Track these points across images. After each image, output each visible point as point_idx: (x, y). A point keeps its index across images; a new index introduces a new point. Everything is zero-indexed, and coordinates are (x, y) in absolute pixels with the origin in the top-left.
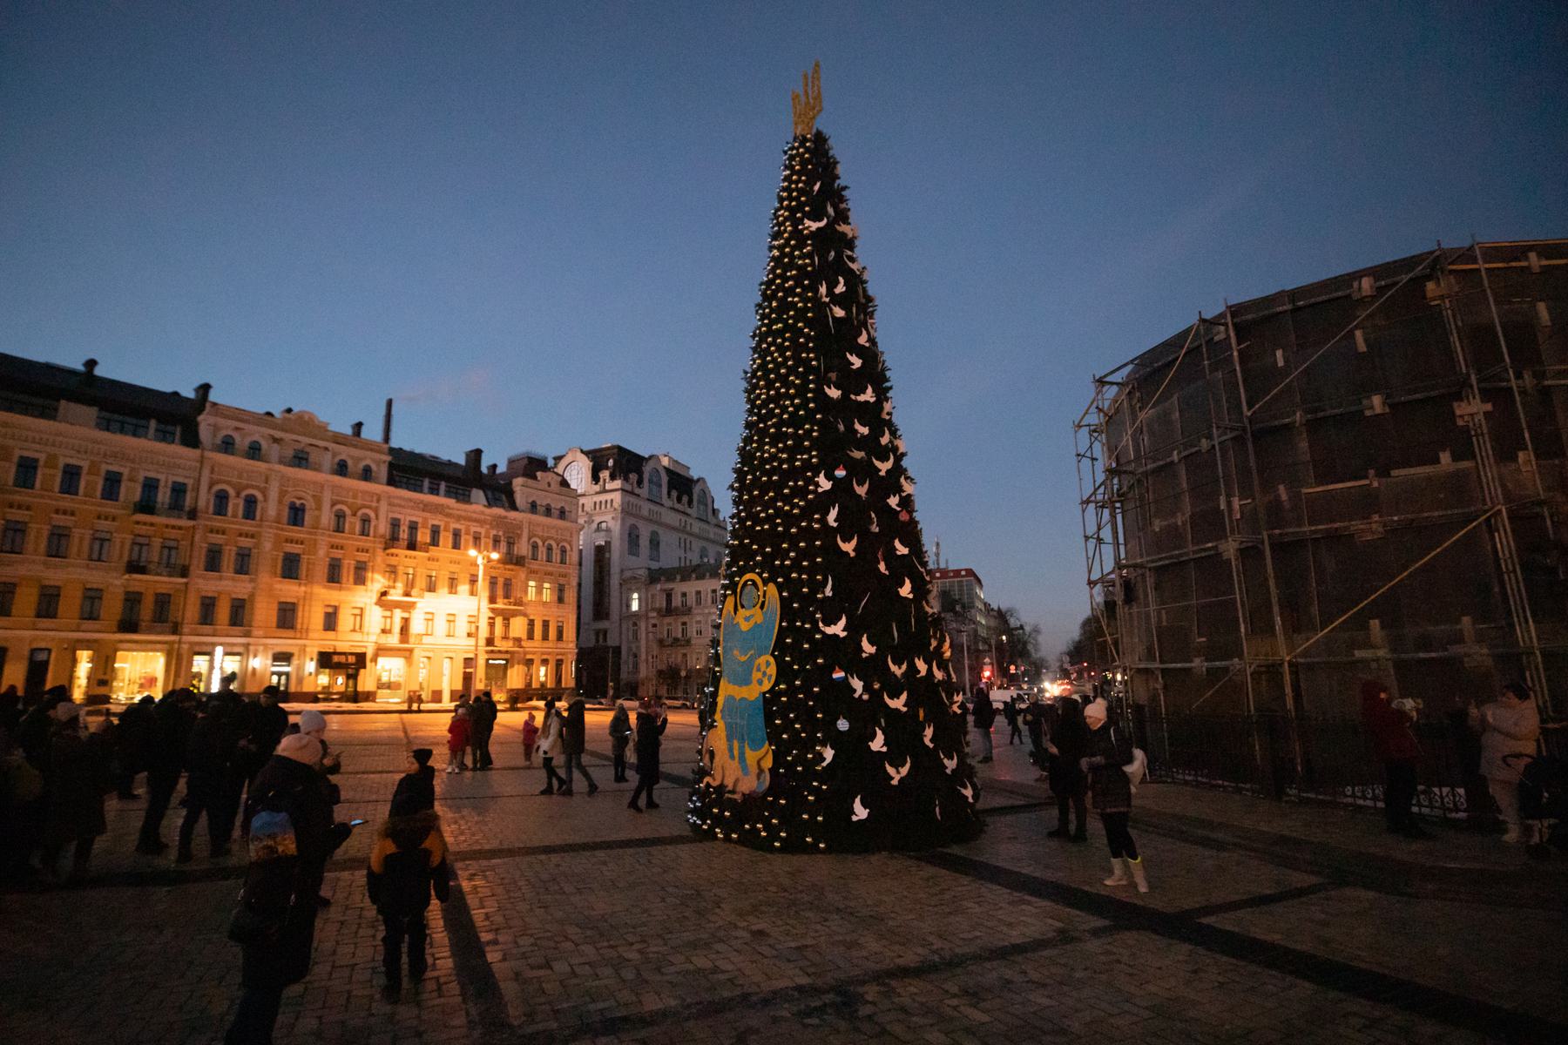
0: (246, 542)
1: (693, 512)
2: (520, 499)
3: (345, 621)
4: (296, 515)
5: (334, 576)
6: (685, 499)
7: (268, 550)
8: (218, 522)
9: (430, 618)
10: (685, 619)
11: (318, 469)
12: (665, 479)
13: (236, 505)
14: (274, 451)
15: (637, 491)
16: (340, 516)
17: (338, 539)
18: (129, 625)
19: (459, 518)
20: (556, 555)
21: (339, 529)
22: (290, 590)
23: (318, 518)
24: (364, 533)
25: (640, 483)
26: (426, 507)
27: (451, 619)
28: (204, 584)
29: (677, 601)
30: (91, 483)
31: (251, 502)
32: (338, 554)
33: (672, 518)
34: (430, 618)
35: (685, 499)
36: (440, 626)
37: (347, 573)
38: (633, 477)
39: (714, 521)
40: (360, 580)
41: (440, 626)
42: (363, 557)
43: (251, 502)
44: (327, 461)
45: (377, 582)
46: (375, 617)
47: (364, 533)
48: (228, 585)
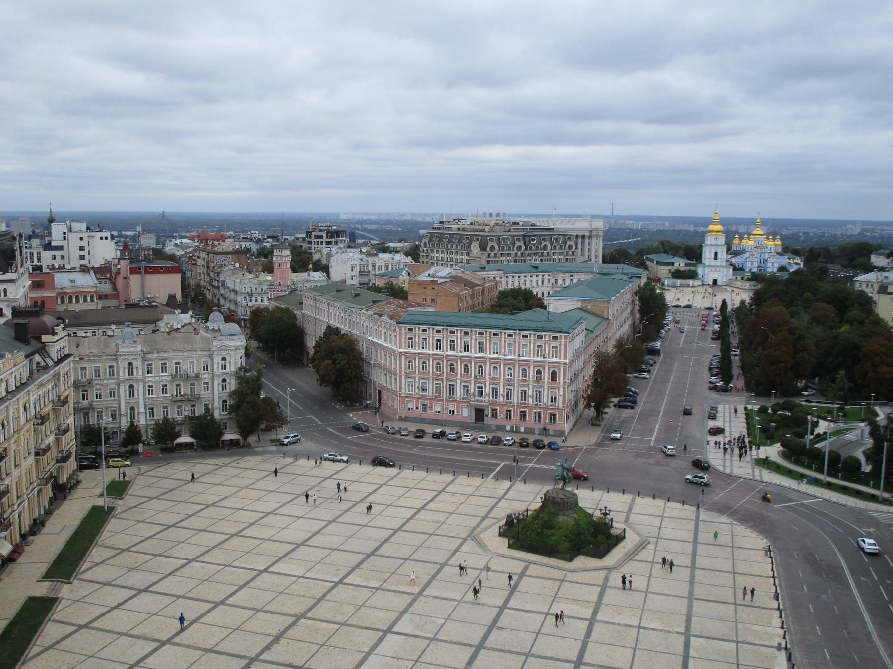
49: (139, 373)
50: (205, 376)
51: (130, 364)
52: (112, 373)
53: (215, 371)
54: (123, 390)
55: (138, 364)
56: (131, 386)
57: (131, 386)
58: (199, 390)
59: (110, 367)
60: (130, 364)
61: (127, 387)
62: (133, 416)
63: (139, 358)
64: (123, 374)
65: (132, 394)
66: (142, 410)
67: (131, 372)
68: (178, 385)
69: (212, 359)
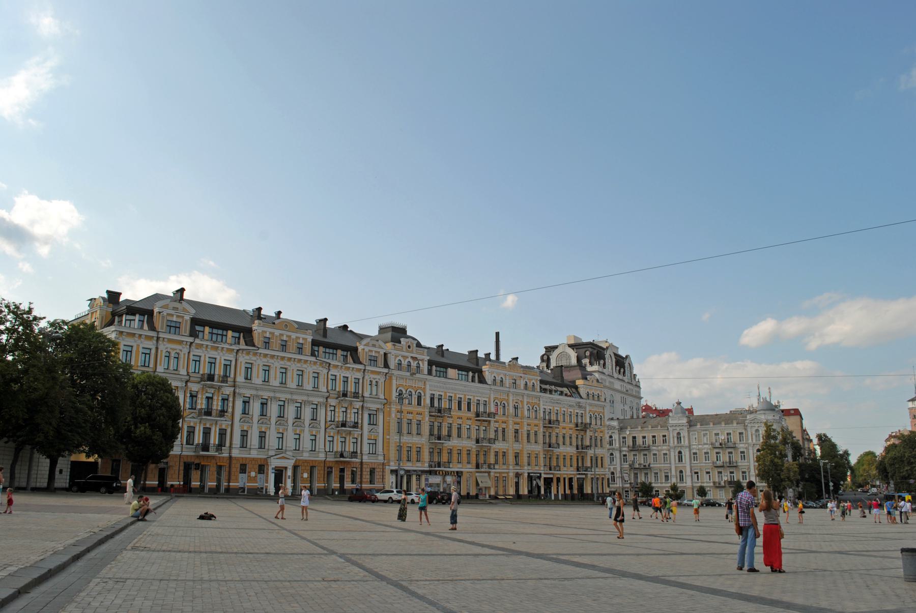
0: (504, 426)
1: (625, 378)
2: (583, 391)
6: (622, 370)
10: (645, 452)
12: (614, 360)
14: (508, 382)
15: (605, 371)
20: (599, 423)
23: (523, 413)
25: (604, 365)
29: (639, 441)
30: (464, 406)
33: (618, 385)
35: (622, 370)
38: (602, 362)
39: (634, 383)
49: (684, 442)
50: (742, 446)
51: (679, 434)
52: (664, 441)
53: (750, 441)
54: (673, 455)
55: (684, 434)
56: (680, 452)
57: (680, 452)
58: (736, 457)
59: (664, 436)
60: (679, 434)
61: (677, 453)
62: (682, 479)
63: (686, 429)
64: (673, 442)
65: (680, 459)
66: (688, 473)
67: (679, 439)
68: (717, 453)
69: (746, 429)
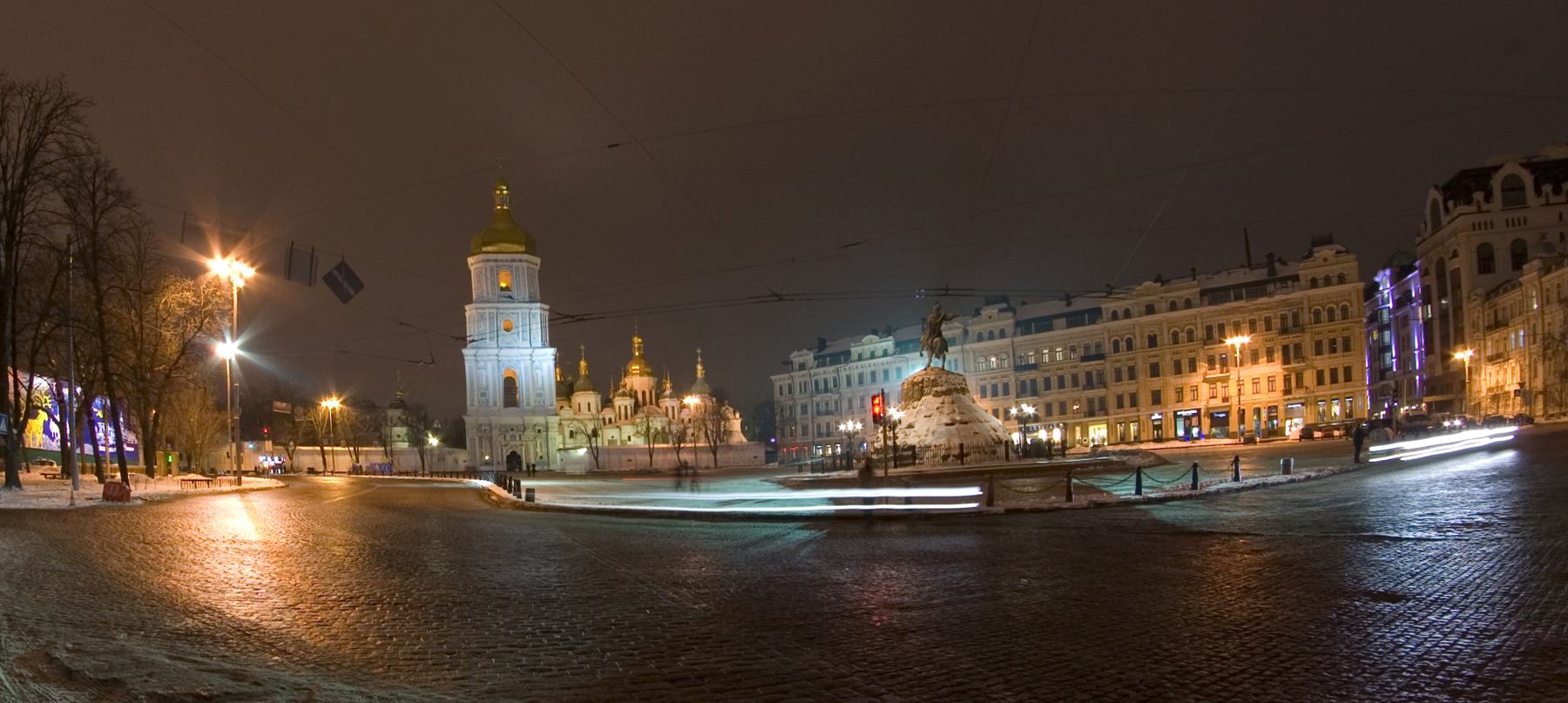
0: (1131, 363)
3: (1188, 396)
4: (1153, 341)
5: (1178, 370)
7: (1142, 367)
8: (1116, 357)
9: (1240, 383)
11: (1160, 311)
13: (1123, 345)
16: (1175, 335)
17: (1177, 348)
18: (1091, 414)
19: (1251, 312)
21: (1176, 342)
22: (1156, 383)
24: (1191, 339)
26: (1227, 312)
27: (1256, 382)
28: (1116, 389)
31: (1129, 342)
32: (1177, 357)
34: (1240, 383)
36: (1248, 388)
37: (1185, 366)
40: (1193, 369)
41: (1248, 388)
42: (1192, 355)
43: (1129, 342)
44: (1164, 306)
45: (1203, 367)
46: (1204, 389)
47: (1191, 339)
48: (1126, 387)
